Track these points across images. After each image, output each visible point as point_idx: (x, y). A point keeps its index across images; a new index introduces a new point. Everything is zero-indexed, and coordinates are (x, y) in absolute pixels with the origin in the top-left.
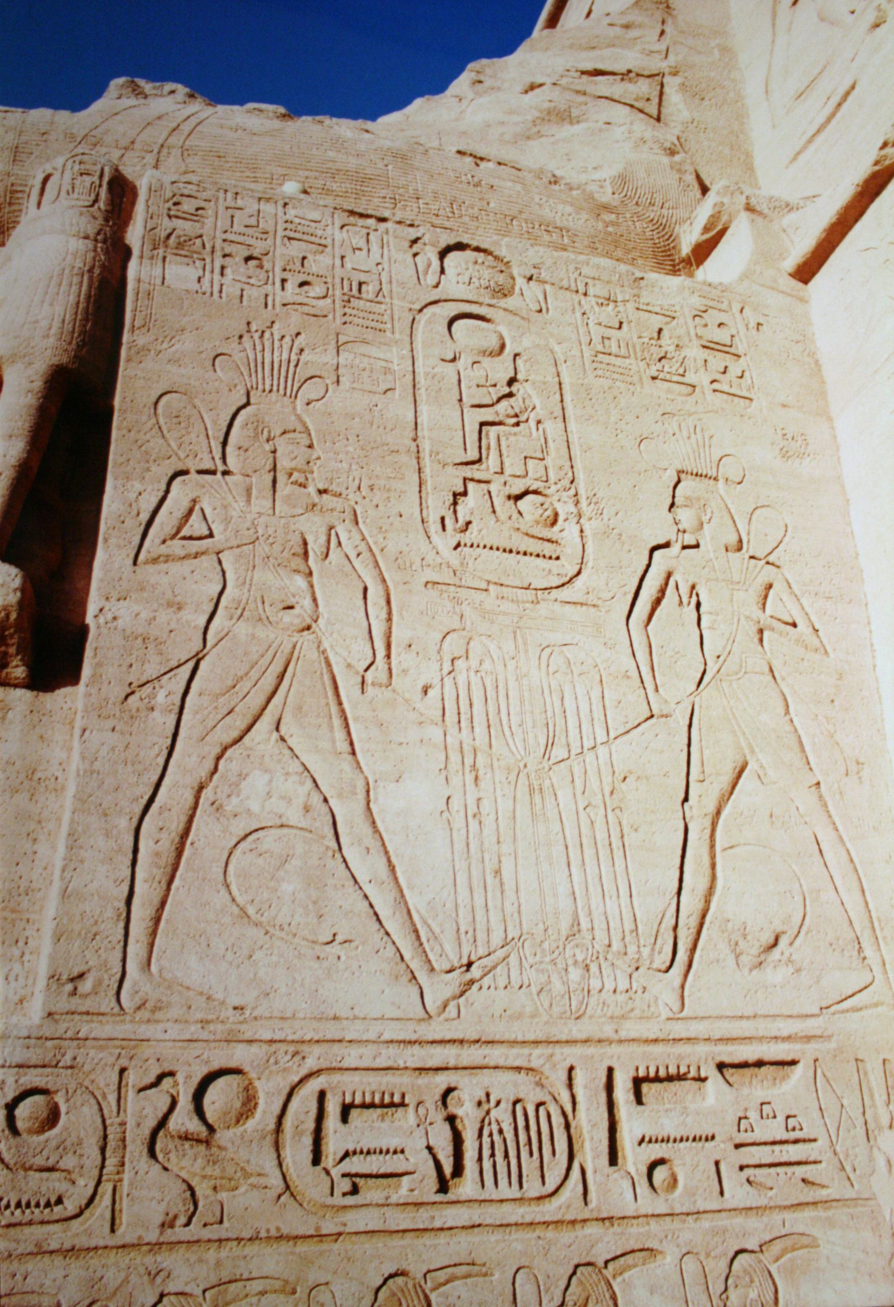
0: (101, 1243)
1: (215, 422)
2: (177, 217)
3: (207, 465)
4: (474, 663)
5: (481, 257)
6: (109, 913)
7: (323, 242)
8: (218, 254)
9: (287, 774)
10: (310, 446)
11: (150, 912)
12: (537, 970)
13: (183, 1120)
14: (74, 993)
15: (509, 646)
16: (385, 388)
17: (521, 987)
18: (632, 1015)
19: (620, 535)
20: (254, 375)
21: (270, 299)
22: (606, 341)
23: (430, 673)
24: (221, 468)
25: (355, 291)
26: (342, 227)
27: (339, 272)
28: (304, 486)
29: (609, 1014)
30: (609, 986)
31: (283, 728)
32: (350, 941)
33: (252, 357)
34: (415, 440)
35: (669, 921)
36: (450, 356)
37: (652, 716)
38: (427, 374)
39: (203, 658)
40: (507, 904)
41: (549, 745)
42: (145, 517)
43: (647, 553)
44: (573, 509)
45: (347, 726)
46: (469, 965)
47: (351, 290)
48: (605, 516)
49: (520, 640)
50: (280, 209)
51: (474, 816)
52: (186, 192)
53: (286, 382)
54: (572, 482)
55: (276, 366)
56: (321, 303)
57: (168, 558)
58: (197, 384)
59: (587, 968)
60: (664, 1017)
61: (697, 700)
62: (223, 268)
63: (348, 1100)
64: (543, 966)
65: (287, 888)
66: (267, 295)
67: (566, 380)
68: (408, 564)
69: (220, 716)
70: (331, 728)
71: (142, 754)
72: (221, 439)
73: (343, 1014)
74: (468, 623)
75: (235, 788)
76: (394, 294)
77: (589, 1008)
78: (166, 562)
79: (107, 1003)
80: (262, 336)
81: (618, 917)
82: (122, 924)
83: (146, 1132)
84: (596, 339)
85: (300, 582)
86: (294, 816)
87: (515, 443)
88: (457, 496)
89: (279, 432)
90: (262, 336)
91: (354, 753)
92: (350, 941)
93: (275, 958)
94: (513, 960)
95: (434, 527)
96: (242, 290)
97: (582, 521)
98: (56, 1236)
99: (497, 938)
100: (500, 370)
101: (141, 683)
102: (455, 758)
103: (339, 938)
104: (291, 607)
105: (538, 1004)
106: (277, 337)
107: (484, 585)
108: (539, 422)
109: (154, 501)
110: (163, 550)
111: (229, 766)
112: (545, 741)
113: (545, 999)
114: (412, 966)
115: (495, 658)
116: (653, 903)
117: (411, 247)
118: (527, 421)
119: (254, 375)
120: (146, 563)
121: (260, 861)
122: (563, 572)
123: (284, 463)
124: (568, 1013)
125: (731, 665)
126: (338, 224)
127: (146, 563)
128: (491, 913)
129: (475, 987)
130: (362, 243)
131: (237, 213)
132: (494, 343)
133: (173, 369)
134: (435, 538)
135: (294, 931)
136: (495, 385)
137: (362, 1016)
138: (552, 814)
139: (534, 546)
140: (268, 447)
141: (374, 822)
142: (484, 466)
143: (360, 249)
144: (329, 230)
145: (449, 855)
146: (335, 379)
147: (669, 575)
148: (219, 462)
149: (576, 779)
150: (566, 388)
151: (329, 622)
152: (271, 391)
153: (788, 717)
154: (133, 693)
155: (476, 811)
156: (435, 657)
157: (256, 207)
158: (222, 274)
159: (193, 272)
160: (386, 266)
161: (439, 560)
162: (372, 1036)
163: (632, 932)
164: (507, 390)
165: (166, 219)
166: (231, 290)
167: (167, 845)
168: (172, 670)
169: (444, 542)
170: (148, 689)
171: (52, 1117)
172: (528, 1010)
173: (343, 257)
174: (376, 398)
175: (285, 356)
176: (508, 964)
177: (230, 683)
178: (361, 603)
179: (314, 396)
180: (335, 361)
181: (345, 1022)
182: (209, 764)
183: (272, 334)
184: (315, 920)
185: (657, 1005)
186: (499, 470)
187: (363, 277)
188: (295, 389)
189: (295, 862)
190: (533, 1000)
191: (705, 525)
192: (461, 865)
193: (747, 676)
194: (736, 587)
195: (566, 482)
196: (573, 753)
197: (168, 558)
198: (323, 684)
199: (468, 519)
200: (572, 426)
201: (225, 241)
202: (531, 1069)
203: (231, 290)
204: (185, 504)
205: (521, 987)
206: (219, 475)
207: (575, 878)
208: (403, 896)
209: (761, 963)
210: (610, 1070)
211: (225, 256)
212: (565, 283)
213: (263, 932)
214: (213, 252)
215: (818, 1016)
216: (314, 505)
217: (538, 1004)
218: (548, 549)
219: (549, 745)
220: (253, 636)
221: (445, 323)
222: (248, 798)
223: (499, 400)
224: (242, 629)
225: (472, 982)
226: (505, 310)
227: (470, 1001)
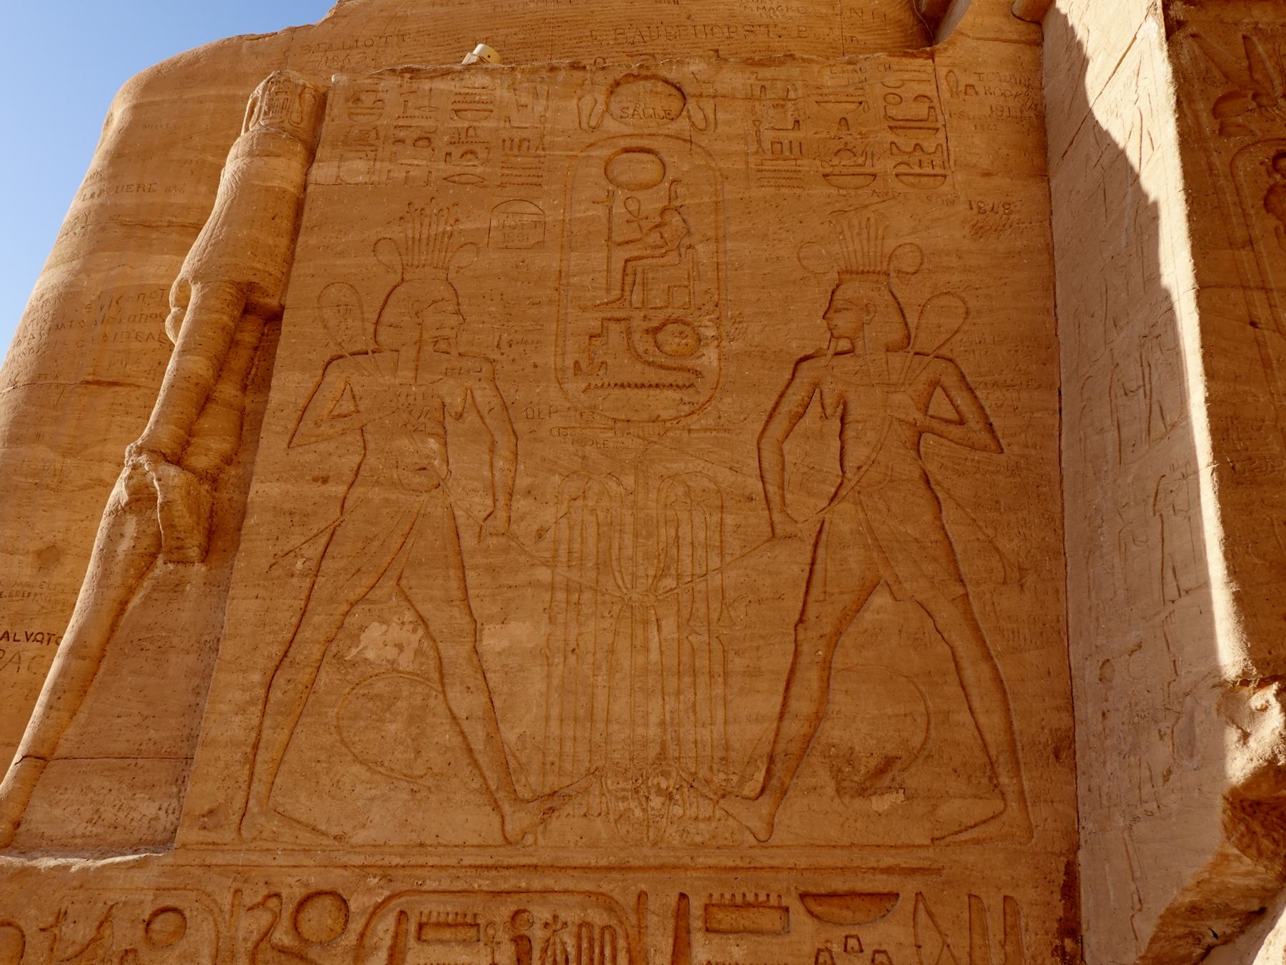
13: (282, 937)
63: (424, 919)
73: (429, 842)
83: (250, 945)
162: (453, 862)
202: (602, 894)
210: (683, 896)
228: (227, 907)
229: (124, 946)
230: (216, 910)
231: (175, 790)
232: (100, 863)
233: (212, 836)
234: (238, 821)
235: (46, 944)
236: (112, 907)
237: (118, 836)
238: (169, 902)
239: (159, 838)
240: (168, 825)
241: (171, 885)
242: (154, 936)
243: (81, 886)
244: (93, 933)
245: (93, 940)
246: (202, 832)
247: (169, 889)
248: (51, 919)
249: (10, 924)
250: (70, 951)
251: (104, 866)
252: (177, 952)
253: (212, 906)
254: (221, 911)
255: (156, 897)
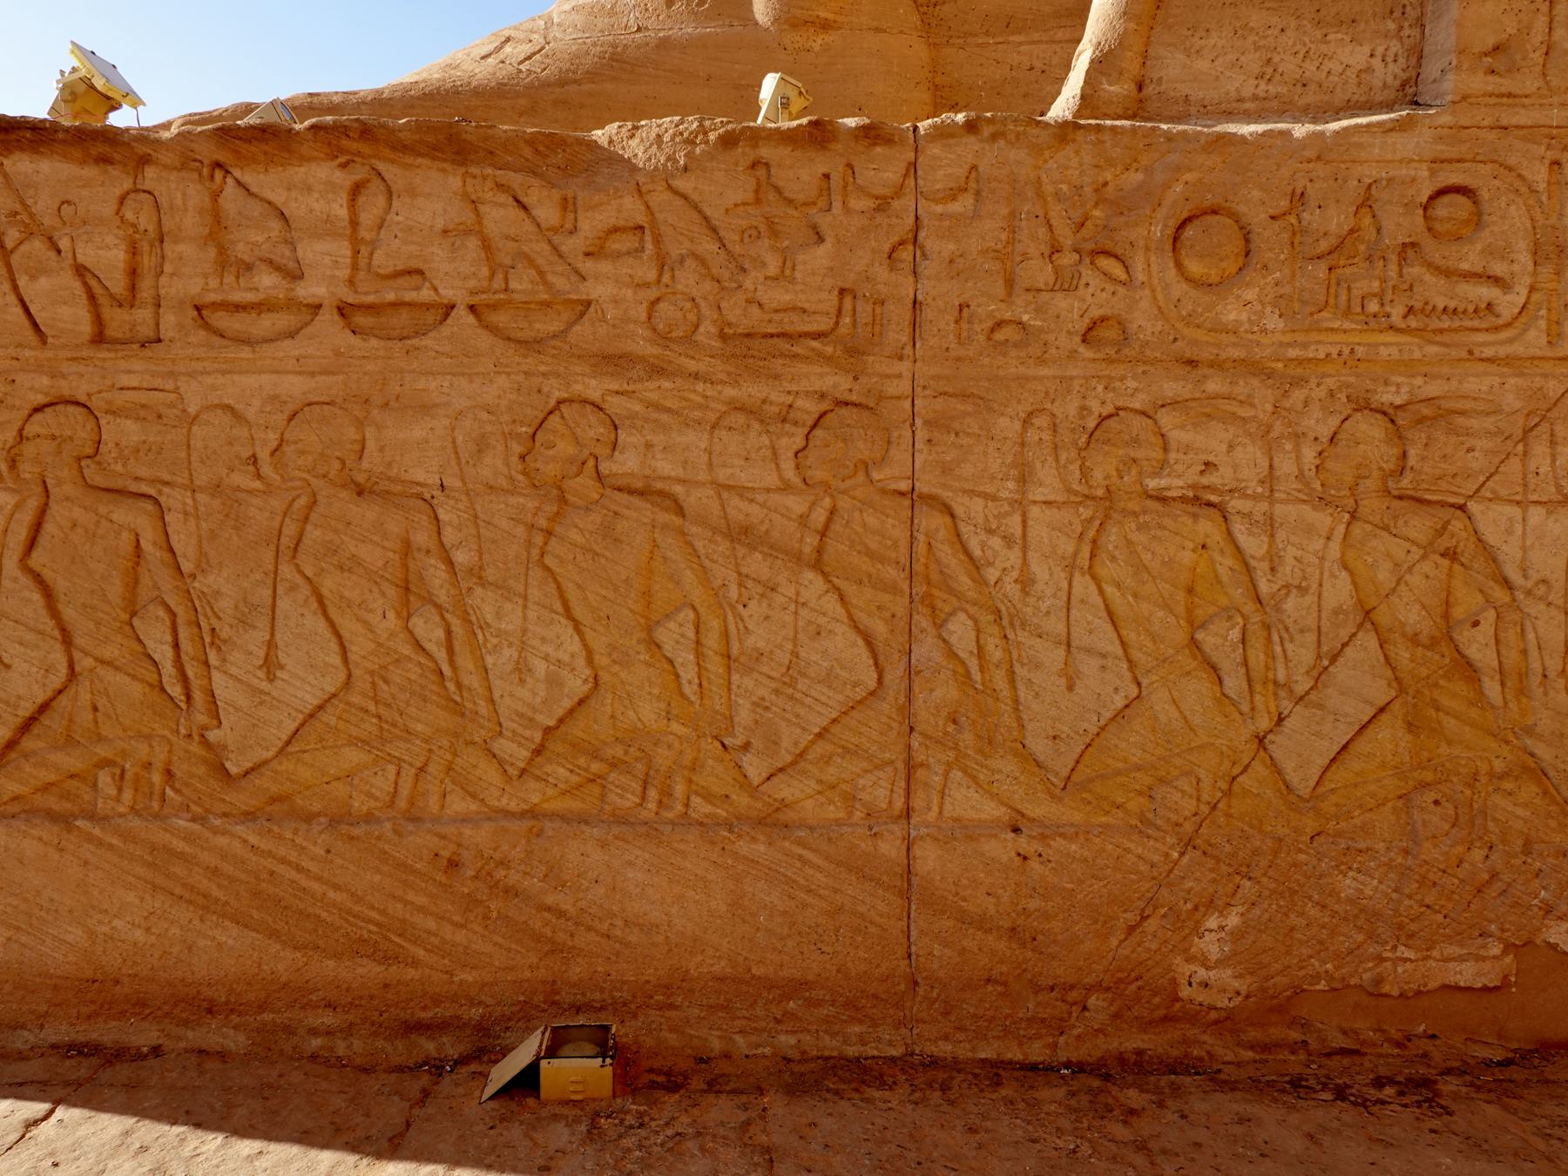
0: (1539, 353)
98: (1486, 342)
171: (1477, 220)
228: (1542, 186)
229: (1401, 239)
230: (1524, 189)
231: (1392, 26)
232: (1335, 126)
233: (1506, 84)
234: (1541, 61)
235: (1285, 236)
236: (1370, 186)
237: (1311, 97)
238: (1455, 179)
239: (1378, 98)
240: (1390, 80)
241: (1454, 156)
242: (1437, 226)
243: (1319, 158)
244: (1351, 222)
245: (1352, 231)
246: (1491, 78)
247: (1450, 161)
248: (1284, 203)
249: (1215, 212)
250: (1324, 245)
251: (1346, 129)
252: (1479, 247)
253: (1518, 184)
254: (1533, 191)
255: (1433, 173)
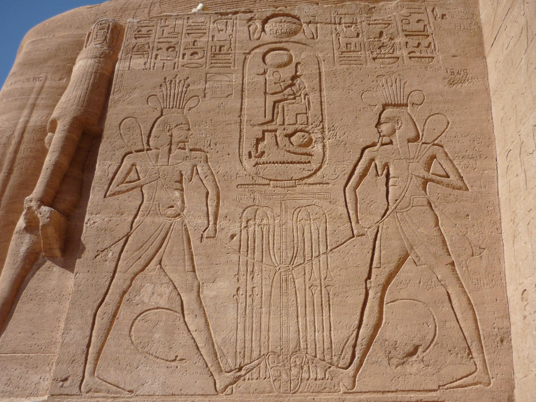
1: (145, 127)
2: (139, 37)
3: (140, 147)
4: (258, 221)
5: (284, 19)
6: (80, 352)
7: (204, 31)
8: (155, 49)
9: (162, 284)
10: (189, 129)
11: (97, 350)
12: (274, 370)
14: (62, 386)
15: (277, 210)
16: (227, 95)
17: (265, 378)
18: (325, 391)
19: (346, 144)
20: (165, 102)
21: (176, 65)
22: (349, 45)
23: (235, 228)
24: (146, 147)
25: (217, 51)
26: (214, 22)
27: (210, 44)
28: (184, 149)
29: (311, 391)
30: (312, 376)
31: (163, 263)
32: (183, 359)
33: (165, 93)
34: (240, 117)
35: (351, 342)
36: (263, 71)
37: (353, 236)
38: (249, 83)
39: (130, 235)
40: (262, 338)
41: (293, 258)
42: (111, 176)
43: (359, 151)
44: (320, 136)
45: (192, 259)
46: (240, 369)
47: (216, 51)
48: (338, 137)
49: (283, 206)
50: (185, 21)
51: (250, 296)
52: (144, 25)
53: (180, 102)
54: (321, 122)
55: (176, 95)
56: (201, 60)
57: (120, 192)
58: (139, 111)
59: (302, 368)
60: (342, 392)
61: (381, 225)
62: (157, 55)
64: (278, 368)
65: (157, 336)
66: (175, 63)
67: (323, 70)
68: (229, 178)
69: (135, 261)
70: (184, 260)
71: (100, 281)
72: (147, 135)
73: (176, 393)
74: (257, 202)
75: (138, 292)
76: (237, 48)
77: (301, 388)
78: (119, 194)
79: (76, 390)
80: (170, 83)
81: (322, 341)
82: (84, 356)
84: (343, 45)
85: (177, 194)
86: (162, 303)
87: (291, 109)
88: (259, 141)
89: (174, 126)
90: (170, 83)
91: (194, 271)
92: (183, 359)
93: (148, 368)
94: (262, 365)
95: (245, 157)
96: (164, 64)
97: (325, 141)
99: (255, 354)
100: (287, 73)
101: (102, 250)
102: (243, 268)
103: (178, 358)
104: (172, 207)
105: (273, 386)
106: (177, 81)
107: (267, 182)
108: (306, 95)
109: (115, 168)
110: (118, 189)
111: (137, 282)
112: (291, 255)
113: (277, 384)
114: (211, 370)
115: (269, 217)
116: (342, 333)
117: (248, 23)
118: (300, 95)
119: (165, 102)
120: (110, 196)
121: (146, 325)
122: (311, 169)
123: (175, 140)
124: (289, 391)
125: (403, 204)
126: (212, 20)
127: (110, 196)
128: (254, 343)
129: (243, 378)
130: (223, 27)
131: (166, 29)
132: (286, 59)
133: (129, 107)
134: (245, 163)
135: (158, 356)
136: (284, 81)
137: (185, 393)
138: (291, 291)
139: (296, 158)
140: (168, 134)
141: (201, 303)
142: (274, 123)
143: (222, 30)
144: (208, 25)
145: (235, 316)
146: (203, 95)
147: (373, 160)
148: (145, 145)
149: (307, 274)
150: (323, 74)
151: (189, 211)
152: (172, 108)
153: (438, 228)
154: (98, 255)
155: (251, 293)
156: (238, 220)
157: (174, 23)
158: (156, 58)
159: (142, 61)
160: (234, 36)
161: (245, 173)
163: (328, 349)
164: (291, 82)
165: (134, 39)
166: (159, 64)
167: (106, 319)
168: (116, 243)
169: (248, 164)
170: (105, 252)
172: (268, 389)
173: (213, 36)
174: (222, 100)
175: (180, 90)
176: (260, 367)
177: (140, 245)
178: (204, 200)
179: (192, 106)
180: (204, 87)
181: (177, 397)
182: (128, 282)
183: (175, 81)
184: (168, 350)
185: (339, 386)
186: (282, 123)
187: (222, 43)
188: (184, 104)
189: (161, 324)
190: (271, 384)
191: (397, 131)
192: (241, 320)
193: (413, 208)
194: (412, 161)
195: (318, 122)
196: (306, 259)
197: (120, 192)
198: (183, 240)
199: (262, 150)
200: (324, 93)
201: (158, 43)
203: (159, 64)
204: (129, 166)
205: (265, 378)
206: (145, 152)
207: (300, 324)
208: (211, 337)
209: (404, 363)
211: (158, 50)
212: (328, 21)
213: (144, 356)
214: (153, 50)
215: (436, 390)
216: (187, 157)
217: (273, 386)
218: (304, 158)
219: (293, 258)
220: (153, 222)
221: (261, 56)
222: (143, 296)
223: (286, 88)
224: (148, 220)
225: (240, 376)
226: (293, 42)
227: (239, 385)
